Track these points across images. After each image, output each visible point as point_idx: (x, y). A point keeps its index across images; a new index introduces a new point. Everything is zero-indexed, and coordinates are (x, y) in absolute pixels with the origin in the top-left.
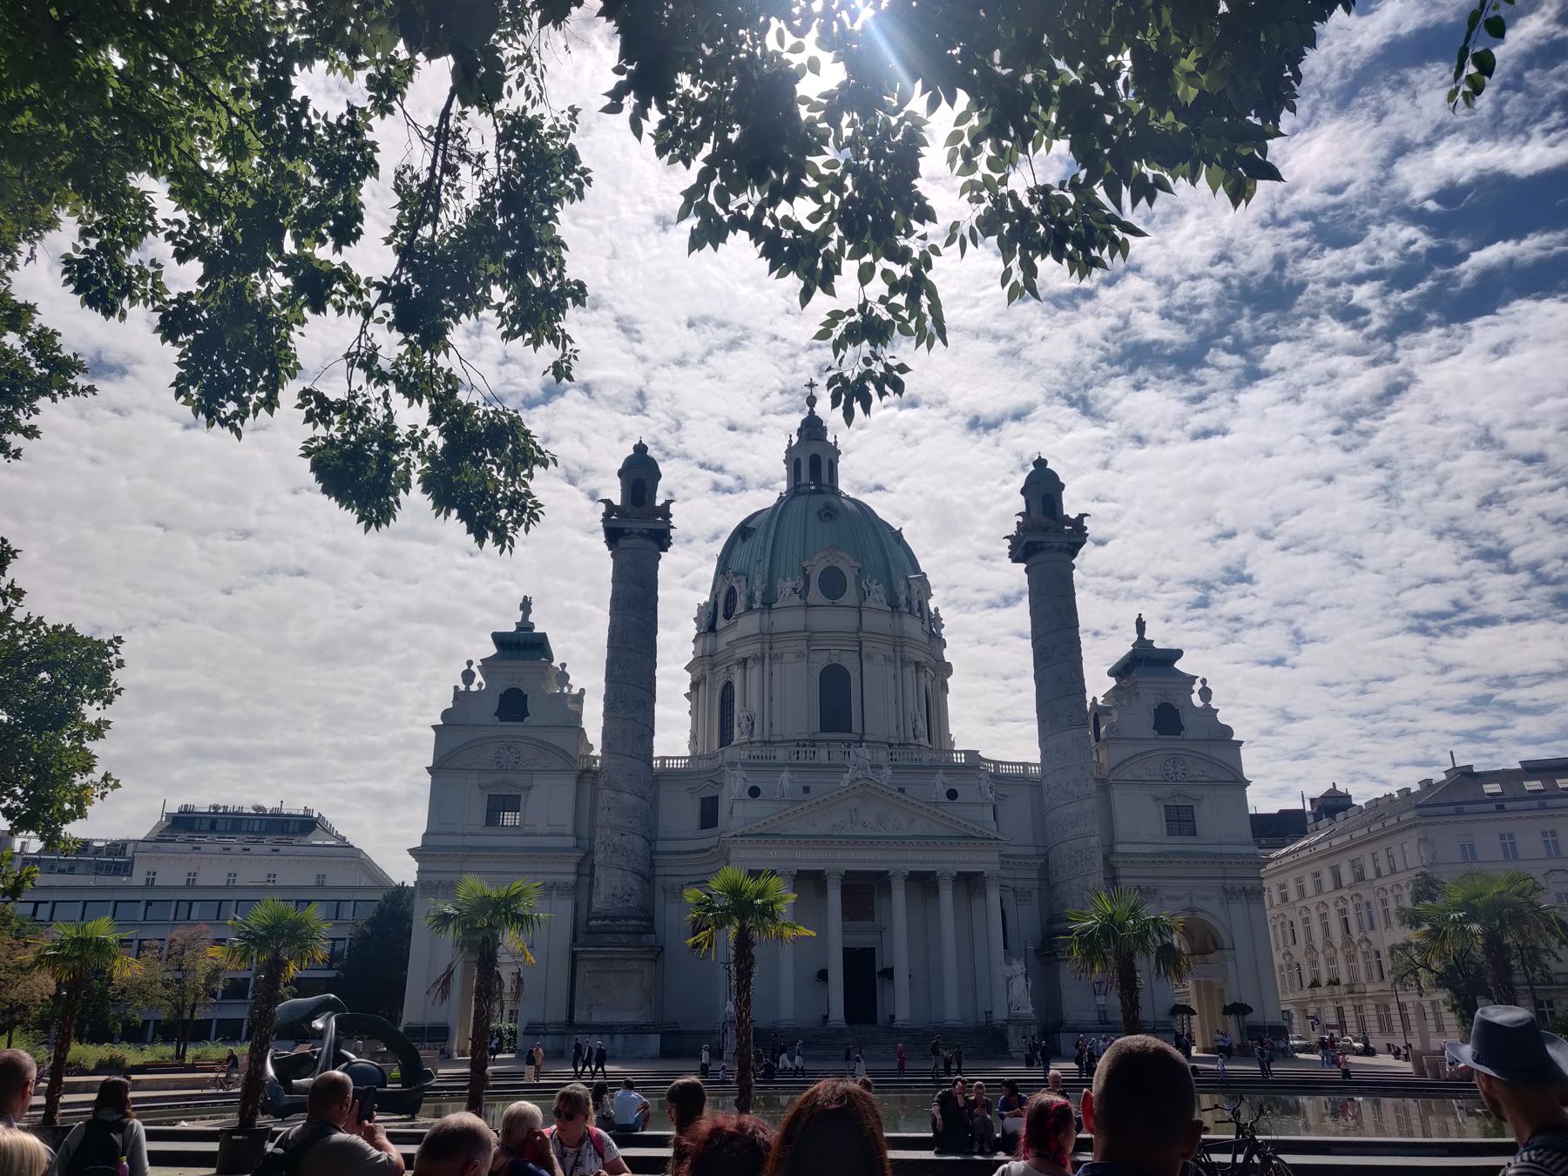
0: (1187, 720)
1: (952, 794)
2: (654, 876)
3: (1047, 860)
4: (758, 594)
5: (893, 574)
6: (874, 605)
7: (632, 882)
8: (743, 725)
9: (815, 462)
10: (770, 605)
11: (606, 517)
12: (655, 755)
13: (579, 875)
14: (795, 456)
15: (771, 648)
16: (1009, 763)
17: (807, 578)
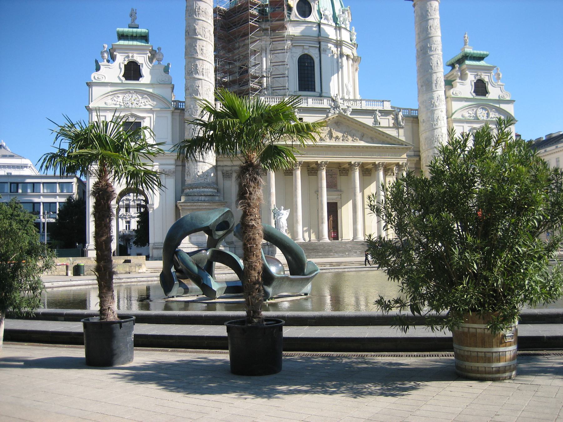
0: (490, 88)
3: (420, 159)
6: (326, 22)
13: (176, 166)
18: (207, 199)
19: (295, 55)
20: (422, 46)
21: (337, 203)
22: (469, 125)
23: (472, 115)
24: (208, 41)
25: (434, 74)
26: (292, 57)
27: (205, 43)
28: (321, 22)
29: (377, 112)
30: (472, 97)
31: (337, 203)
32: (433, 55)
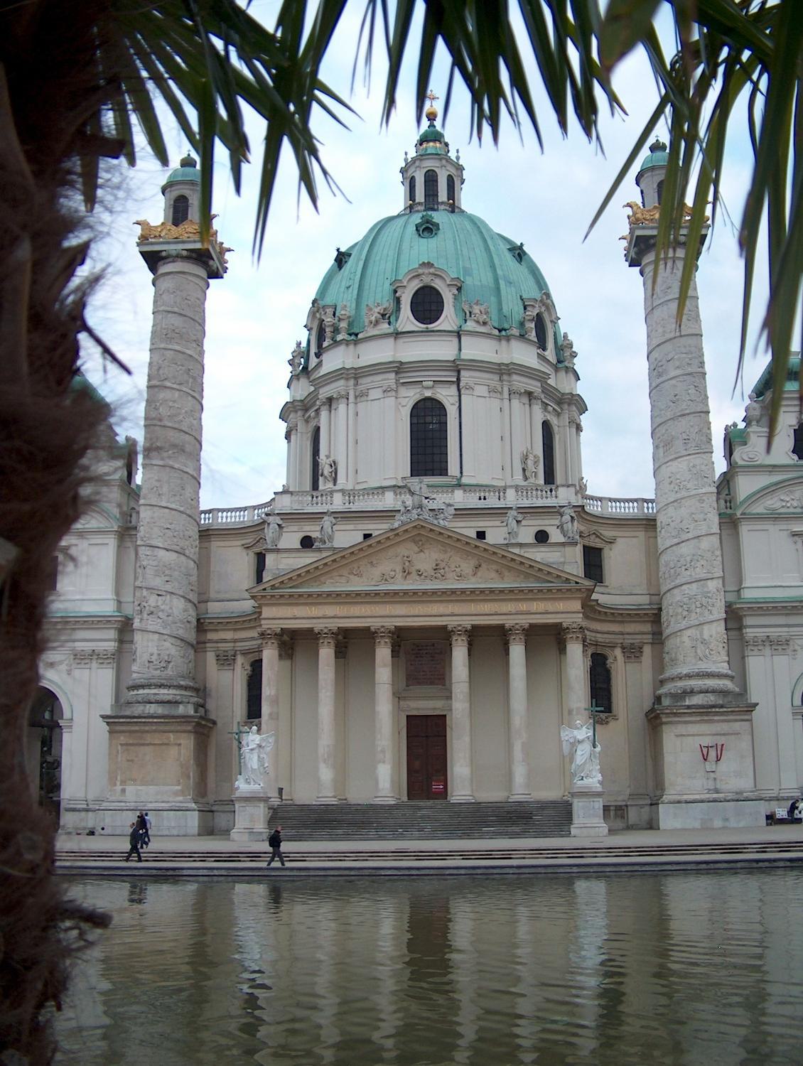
1: (542, 537)
2: (205, 643)
3: (660, 609)
4: (343, 325)
5: (503, 292)
7: (171, 649)
8: (326, 473)
9: (431, 179)
10: (356, 335)
11: (143, 239)
12: (204, 506)
13: (121, 641)
14: (410, 174)
15: (356, 384)
16: (616, 500)
17: (398, 301)
18: (159, 710)
19: (404, 401)
20: (656, 360)
21: (445, 716)
22: (784, 527)
23: (789, 505)
24: (184, 389)
25: (680, 419)
26: (397, 410)
27: (177, 394)
28: (463, 328)
29: (513, 513)
30: (791, 462)
31: (445, 716)
32: (676, 377)
